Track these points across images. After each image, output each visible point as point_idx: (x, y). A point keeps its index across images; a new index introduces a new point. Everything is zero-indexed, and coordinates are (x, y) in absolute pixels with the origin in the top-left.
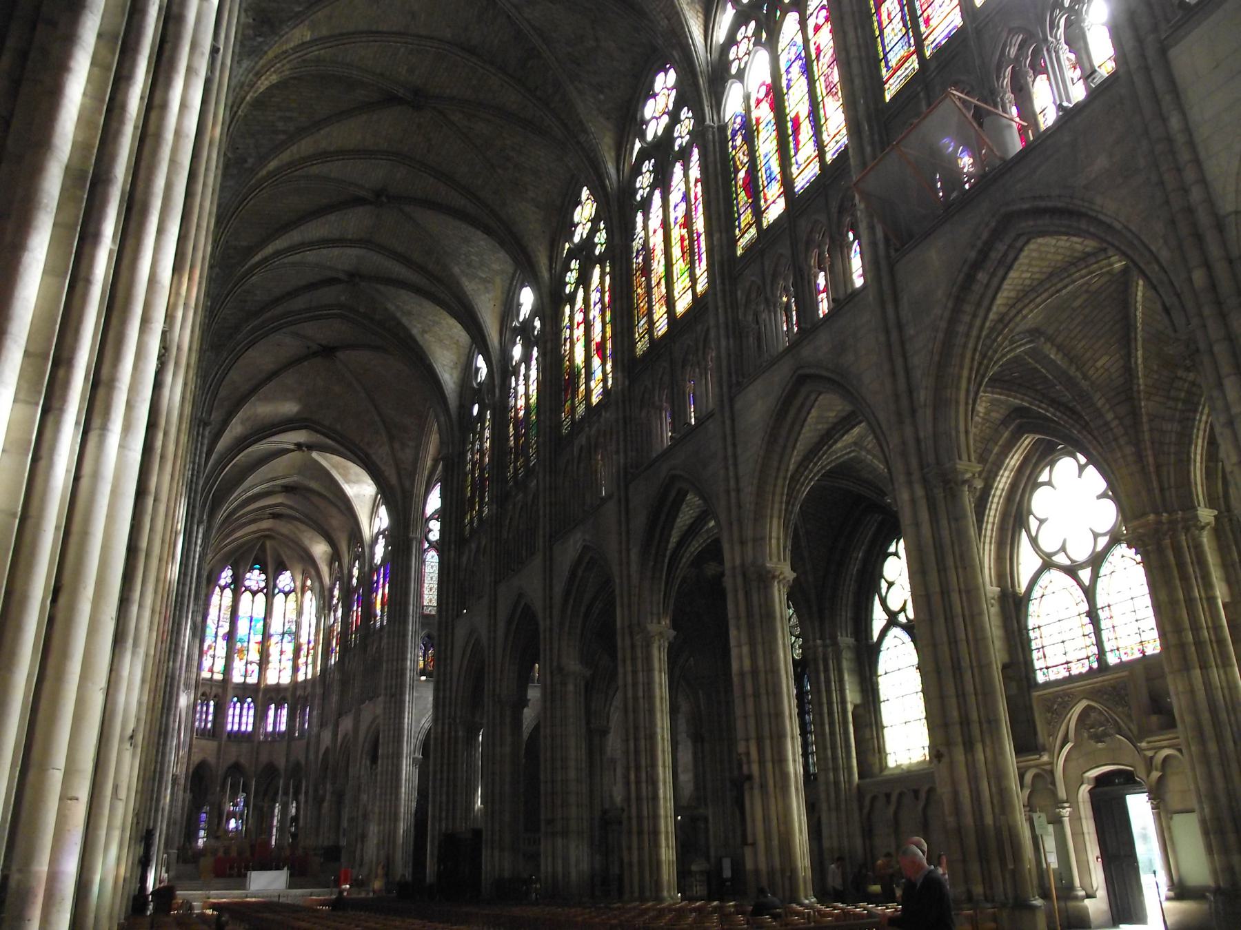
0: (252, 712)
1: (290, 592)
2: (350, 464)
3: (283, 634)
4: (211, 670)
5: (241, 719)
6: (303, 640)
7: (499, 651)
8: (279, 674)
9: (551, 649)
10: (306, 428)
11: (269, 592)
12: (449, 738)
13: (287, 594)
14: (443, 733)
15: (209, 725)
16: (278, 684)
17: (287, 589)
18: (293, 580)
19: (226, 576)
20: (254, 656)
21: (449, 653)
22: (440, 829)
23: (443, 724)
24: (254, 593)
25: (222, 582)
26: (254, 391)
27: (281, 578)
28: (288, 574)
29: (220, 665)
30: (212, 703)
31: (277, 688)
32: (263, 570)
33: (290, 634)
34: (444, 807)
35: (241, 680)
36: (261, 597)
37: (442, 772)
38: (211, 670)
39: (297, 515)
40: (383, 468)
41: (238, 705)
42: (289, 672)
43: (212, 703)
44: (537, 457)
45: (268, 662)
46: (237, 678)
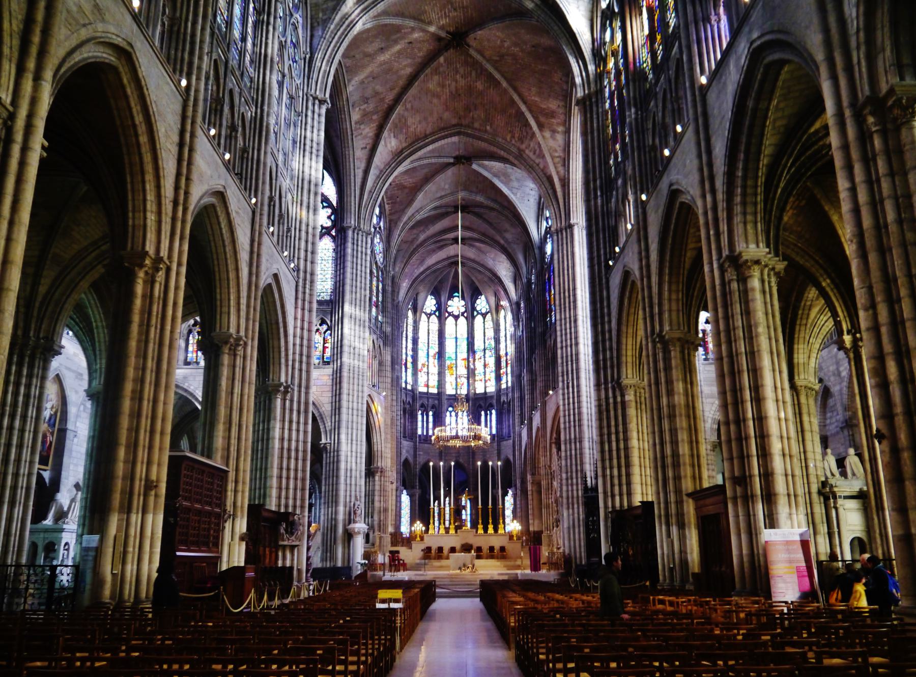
1: (487, 313)
2: (509, 168)
3: (485, 350)
4: (427, 386)
5: (457, 424)
6: (502, 353)
7: (654, 279)
8: (485, 385)
9: (718, 234)
10: (458, 134)
11: (470, 314)
12: (615, 403)
13: (484, 315)
14: (607, 398)
16: (485, 393)
17: (484, 311)
18: (488, 302)
19: (430, 304)
20: (463, 371)
21: (606, 310)
22: (613, 506)
23: (606, 390)
24: (456, 318)
25: (429, 312)
26: (397, 100)
27: (478, 301)
28: (483, 297)
29: (434, 381)
30: (431, 413)
31: (485, 396)
34: (616, 481)
35: (453, 392)
36: (462, 321)
37: (610, 442)
38: (427, 386)
39: (475, 235)
40: (537, 161)
41: (453, 414)
43: (431, 413)
44: (677, 16)
46: (450, 390)
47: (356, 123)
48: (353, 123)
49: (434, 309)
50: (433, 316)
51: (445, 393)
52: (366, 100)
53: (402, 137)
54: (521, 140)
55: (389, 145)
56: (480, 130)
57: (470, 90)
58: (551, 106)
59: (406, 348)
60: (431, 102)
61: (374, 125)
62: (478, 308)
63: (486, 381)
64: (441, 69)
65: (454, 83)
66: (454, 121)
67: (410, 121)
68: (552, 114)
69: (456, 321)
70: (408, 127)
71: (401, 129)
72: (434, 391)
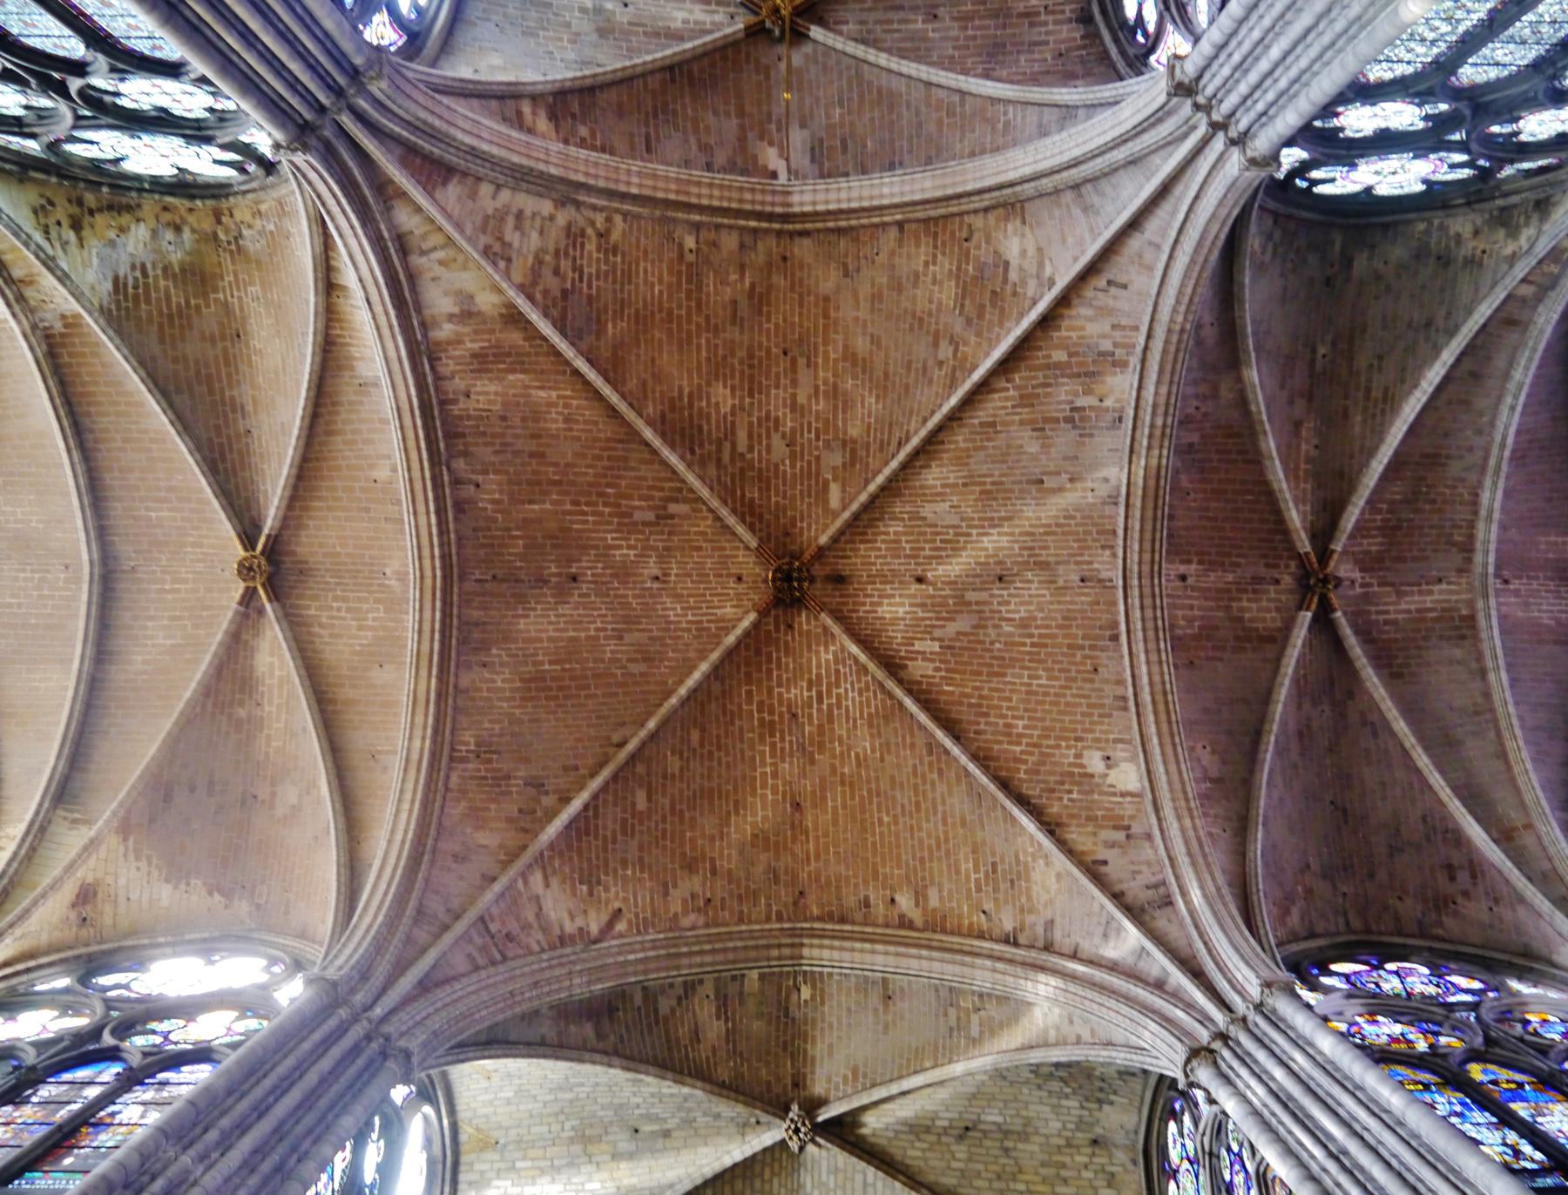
47: (1123, 365)
48: (1134, 361)
52: (1076, 419)
53: (983, 253)
54: (574, 236)
55: (1031, 251)
56: (718, 227)
57: (753, 382)
58: (493, 388)
60: (875, 340)
61: (1066, 331)
64: (836, 459)
65: (802, 399)
66: (803, 249)
67: (947, 294)
68: (482, 362)
70: (957, 275)
71: (979, 279)
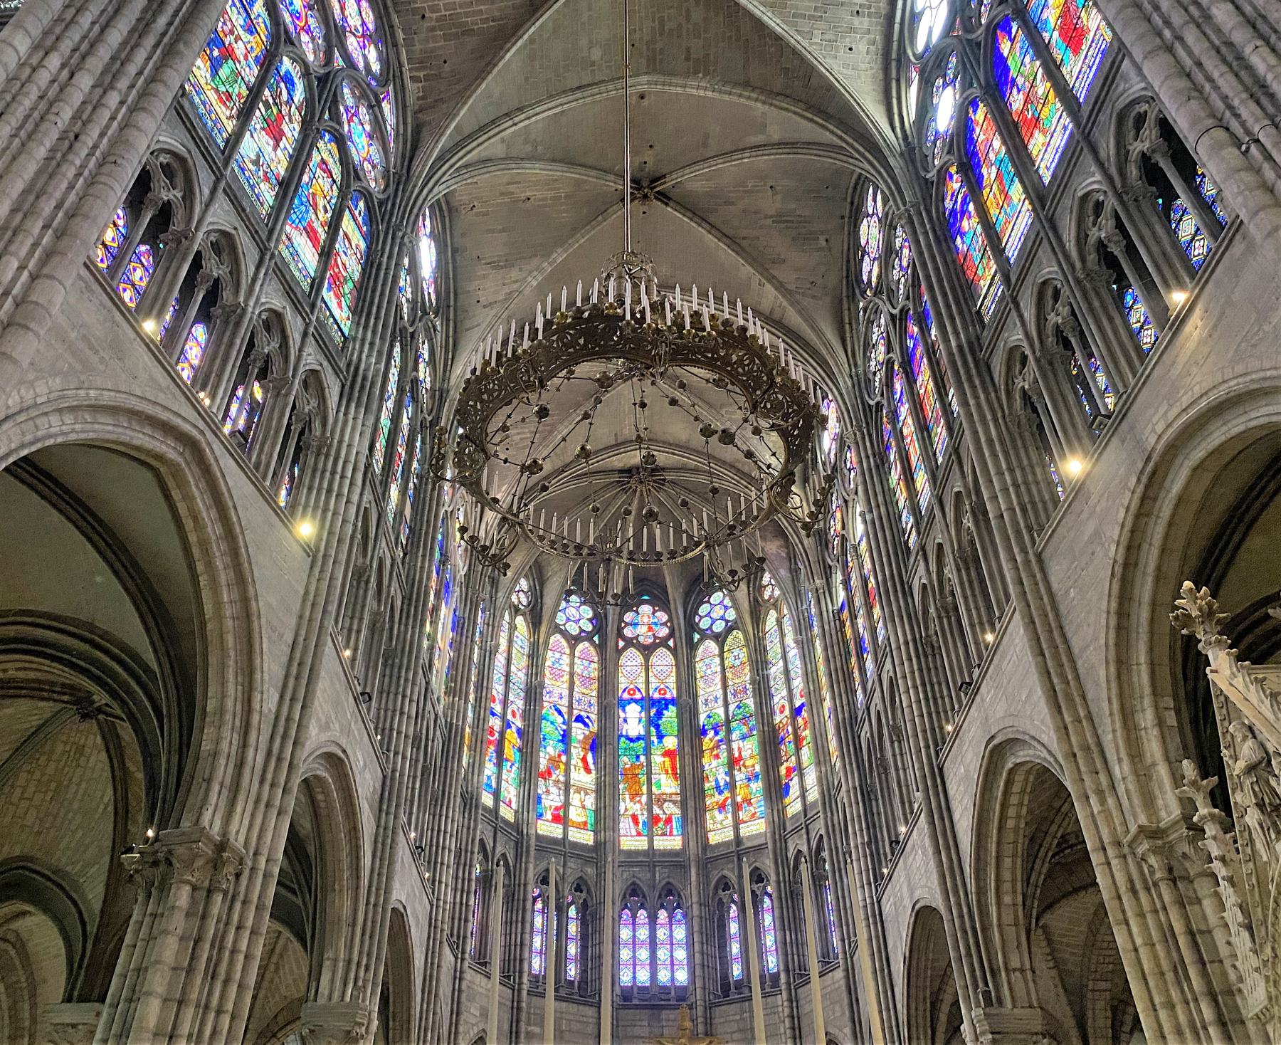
0: (680, 933)
1: (729, 630)
3: (728, 721)
11: (684, 638)
13: (720, 639)
15: (572, 971)
16: (738, 840)
17: (719, 627)
20: (667, 785)
24: (647, 651)
25: (573, 629)
27: (704, 609)
28: (717, 597)
29: (582, 808)
31: (738, 849)
32: (661, 601)
33: (745, 720)
35: (642, 844)
36: (663, 660)
42: (759, 805)
43: (572, 912)
45: (701, 794)
49: (589, 627)
50: (587, 644)
51: (615, 843)
59: (505, 703)
62: (705, 624)
63: (737, 807)
69: (647, 659)
72: (587, 838)
